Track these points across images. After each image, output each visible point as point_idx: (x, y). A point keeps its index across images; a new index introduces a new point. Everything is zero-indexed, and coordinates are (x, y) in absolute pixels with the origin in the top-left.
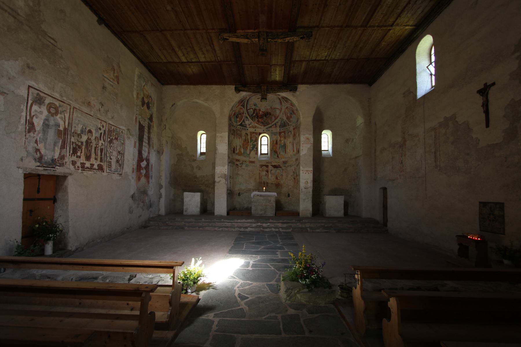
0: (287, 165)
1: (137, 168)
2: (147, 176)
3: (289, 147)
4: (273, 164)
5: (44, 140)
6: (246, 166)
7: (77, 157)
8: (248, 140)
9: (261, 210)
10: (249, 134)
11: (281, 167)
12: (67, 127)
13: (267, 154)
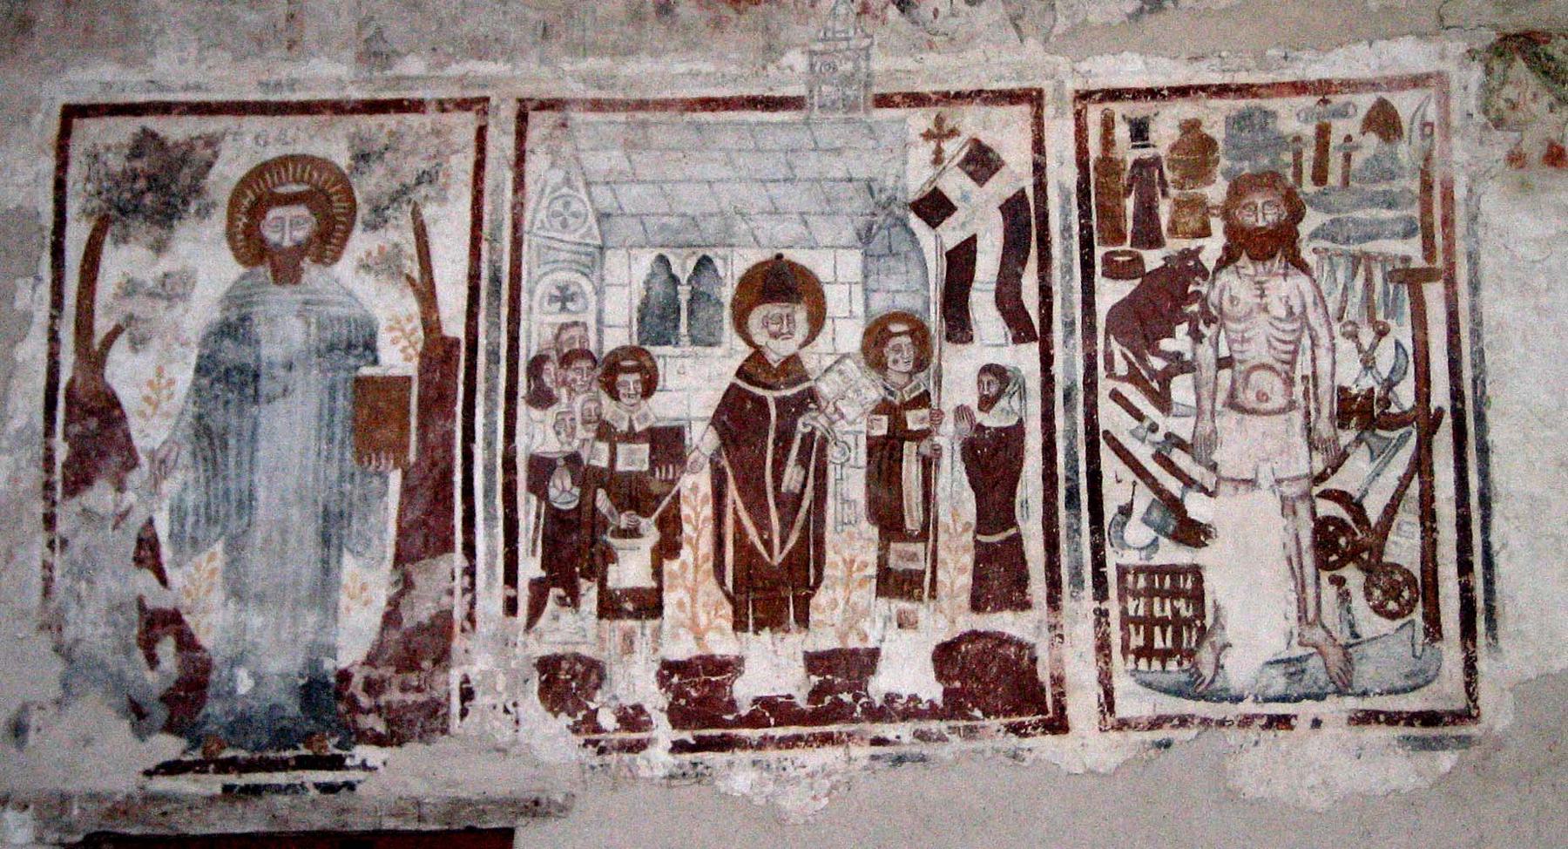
5: (226, 513)
7: (609, 607)
12: (455, 327)
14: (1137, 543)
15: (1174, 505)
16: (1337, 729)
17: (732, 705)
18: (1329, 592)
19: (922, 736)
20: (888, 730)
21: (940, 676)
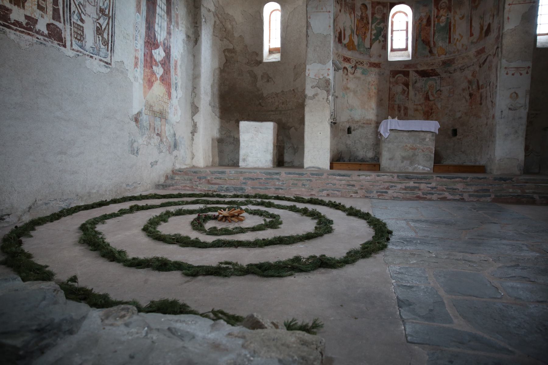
0: (451, 69)
1: (146, 60)
2: (166, 80)
3: (461, 29)
4: (420, 68)
6: (363, 73)
8: (367, 18)
9: (404, 158)
10: (369, 6)
11: (437, 75)
13: (406, 49)
14: (75, 18)
15: (80, 14)
16: (97, 61)
17: (9, 19)
18: (98, 39)
19: (45, 40)
20: (40, 37)
21: (47, 30)
